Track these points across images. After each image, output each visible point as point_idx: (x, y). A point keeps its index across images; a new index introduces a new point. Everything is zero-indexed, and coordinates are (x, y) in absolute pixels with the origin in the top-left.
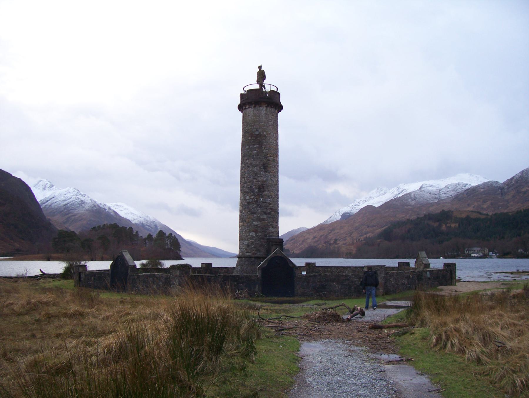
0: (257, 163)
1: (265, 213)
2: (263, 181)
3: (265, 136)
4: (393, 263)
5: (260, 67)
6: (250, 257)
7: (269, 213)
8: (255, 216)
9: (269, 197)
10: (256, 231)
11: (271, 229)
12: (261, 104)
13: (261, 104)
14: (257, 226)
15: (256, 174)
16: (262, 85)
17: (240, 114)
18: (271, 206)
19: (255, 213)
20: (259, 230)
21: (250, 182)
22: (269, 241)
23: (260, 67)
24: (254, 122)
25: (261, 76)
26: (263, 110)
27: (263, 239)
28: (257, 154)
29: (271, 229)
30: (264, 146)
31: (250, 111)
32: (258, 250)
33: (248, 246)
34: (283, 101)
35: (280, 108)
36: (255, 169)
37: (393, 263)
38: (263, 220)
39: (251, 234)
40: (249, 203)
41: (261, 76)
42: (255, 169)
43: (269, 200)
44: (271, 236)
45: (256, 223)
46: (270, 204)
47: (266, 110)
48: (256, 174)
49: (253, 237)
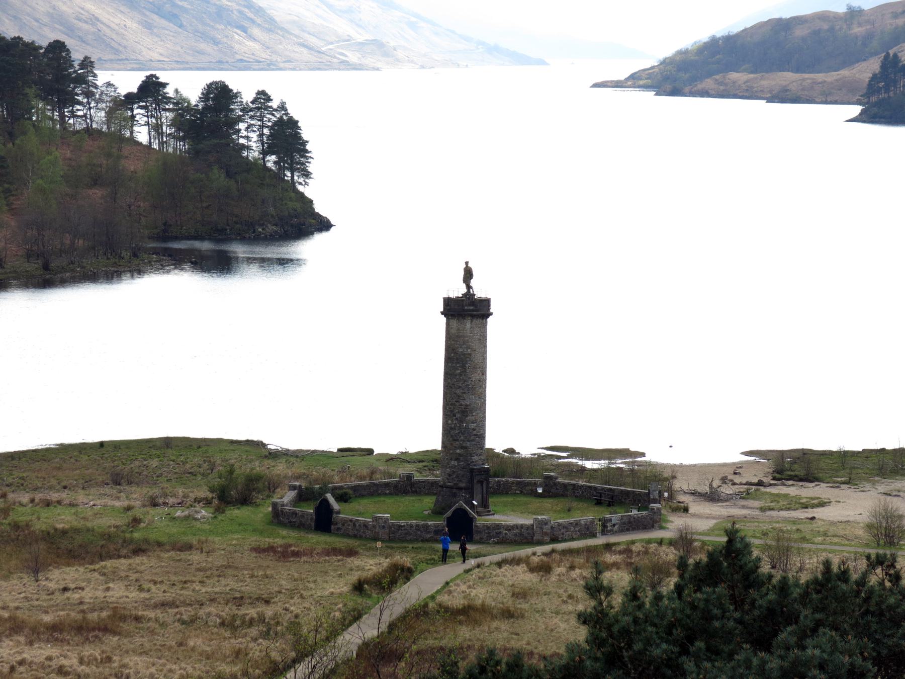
2: (467, 405)
3: (470, 354)
5: (467, 263)
6: (451, 488)
7: (473, 440)
10: (457, 459)
12: (466, 314)
14: (459, 454)
15: (459, 397)
16: (469, 287)
17: (443, 319)
18: (475, 432)
20: (461, 458)
22: (472, 471)
23: (467, 263)
25: (468, 274)
26: (468, 324)
28: (460, 375)
31: (454, 323)
33: (450, 475)
36: (459, 392)
38: (465, 448)
39: (453, 462)
40: (451, 428)
42: (459, 392)
43: (473, 426)
45: (458, 451)
46: (474, 430)
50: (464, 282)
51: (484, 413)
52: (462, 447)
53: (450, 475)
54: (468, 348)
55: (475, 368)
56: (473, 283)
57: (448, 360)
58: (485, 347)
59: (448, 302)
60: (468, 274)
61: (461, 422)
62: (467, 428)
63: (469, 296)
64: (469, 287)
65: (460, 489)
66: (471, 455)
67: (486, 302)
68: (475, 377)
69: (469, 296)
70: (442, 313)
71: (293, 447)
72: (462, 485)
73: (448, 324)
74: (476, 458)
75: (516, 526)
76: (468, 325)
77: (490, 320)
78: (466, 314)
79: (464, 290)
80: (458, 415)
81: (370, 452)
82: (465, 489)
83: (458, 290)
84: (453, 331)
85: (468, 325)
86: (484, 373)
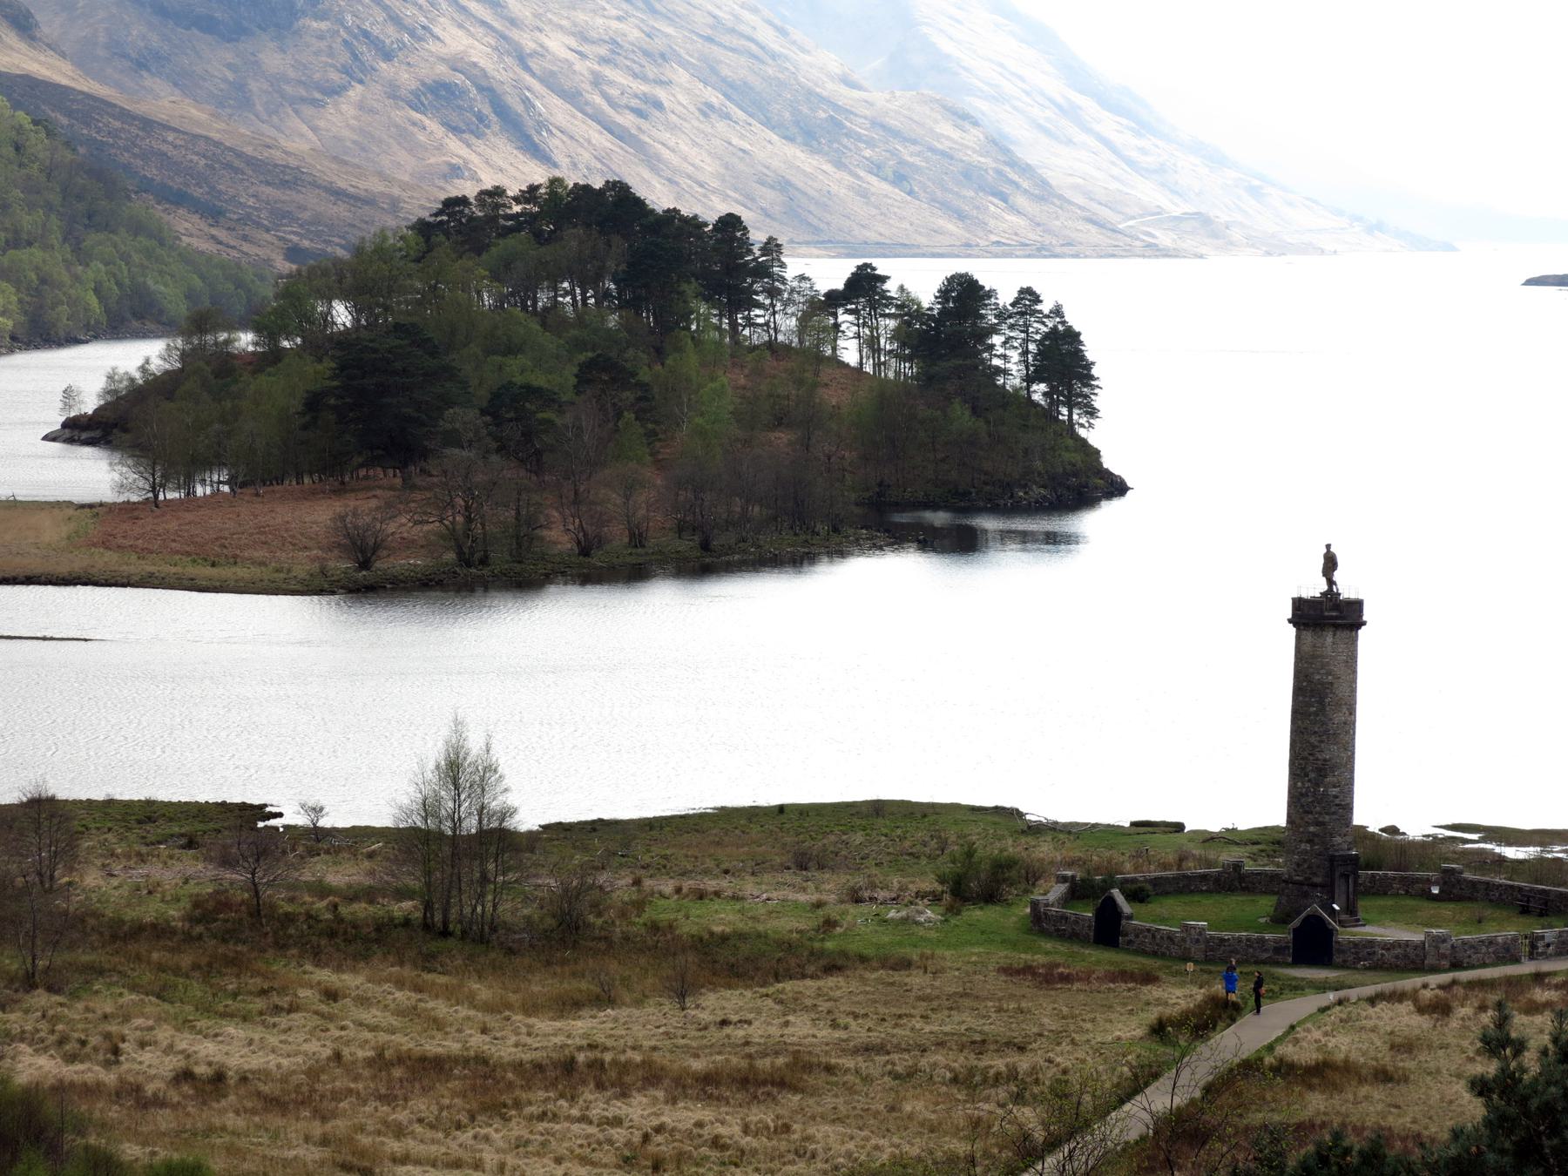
5: (1328, 546)
6: (1301, 884)
10: (1309, 841)
12: (1327, 622)
13: (1327, 622)
14: (1314, 834)
15: (1314, 747)
16: (1331, 582)
17: (1292, 630)
22: (1332, 859)
23: (1328, 546)
24: (1314, 657)
25: (1330, 564)
31: (1308, 636)
32: (1315, 874)
33: (1298, 865)
36: (1313, 739)
39: (1303, 846)
42: (1313, 739)
43: (1334, 791)
45: (1312, 829)
49: (1306, 852)
50: (1325, 574)
51: (1352, 771)
52: (1318, 824)
53: (1298, 865)
54: (1328, 673)
55: (1338, 705)
56: (1337, 576)
57: (1298, 691)
58: (1355, 672)
59: (1299, 604)
60: (1330, 564)
61: (1317, 785)
62: (1325, 794)
63: (1331, 596)
64: (1331, 582)
65: (1315, 886)
66: (1332, 835)
67: (1357, 606)
68: (1339, 718)
69: (1331, 596)
70: (1290, 621)
71: (1063, 817)
72: (1317, 880)
73: (1298, 638)
74: (1338, 839)
75: (1397, 944)
76: (1329, 640)
77: (1362, 633)
78: (1327, 622)
79: (1322, 586)
80: (1312, 775)
81: (1179, 827)
82: (1322, 886)
83: (1314, 587)
84: (1306, 648)
85: (1329, 640)
86: (1352, 711)
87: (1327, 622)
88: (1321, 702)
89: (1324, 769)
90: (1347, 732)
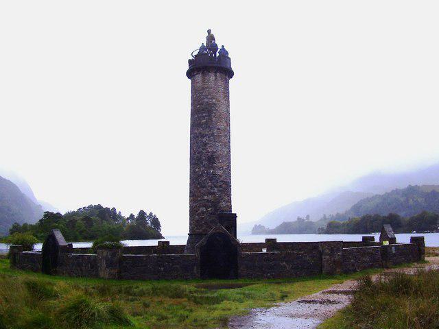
0: (207, 133)
1: (216, 187)
2: (213, 152)
4: (358, 238)
5: (209, 31)
8: (204, 189)
9: (219, 169)
11: (223, 204)
14: (208, 201)
15: (206, 144)
17: (190, 81)
19: (205, 186)
21: (199, 153)
23: (209, 31)
27: (214, 214)
28: (206, 123)
29: (223, 204)
30: (213, 115)
31: (199, 77)
33: (197, 221)
34: (234, 67)
35: (230, 74)
37: (358, 238)
38: (214, 194)
39: (201, 209)
41: (211, 38)
43: (220, 172)
44: (223, 211)
47: (216, 76)
48: (206, 144)
49: (203, 213)
54: (212, 98)
57: (194, 112)
87: (210, 67)
88: (209, 116)
89: (212, 159)
90: (226, 136)
